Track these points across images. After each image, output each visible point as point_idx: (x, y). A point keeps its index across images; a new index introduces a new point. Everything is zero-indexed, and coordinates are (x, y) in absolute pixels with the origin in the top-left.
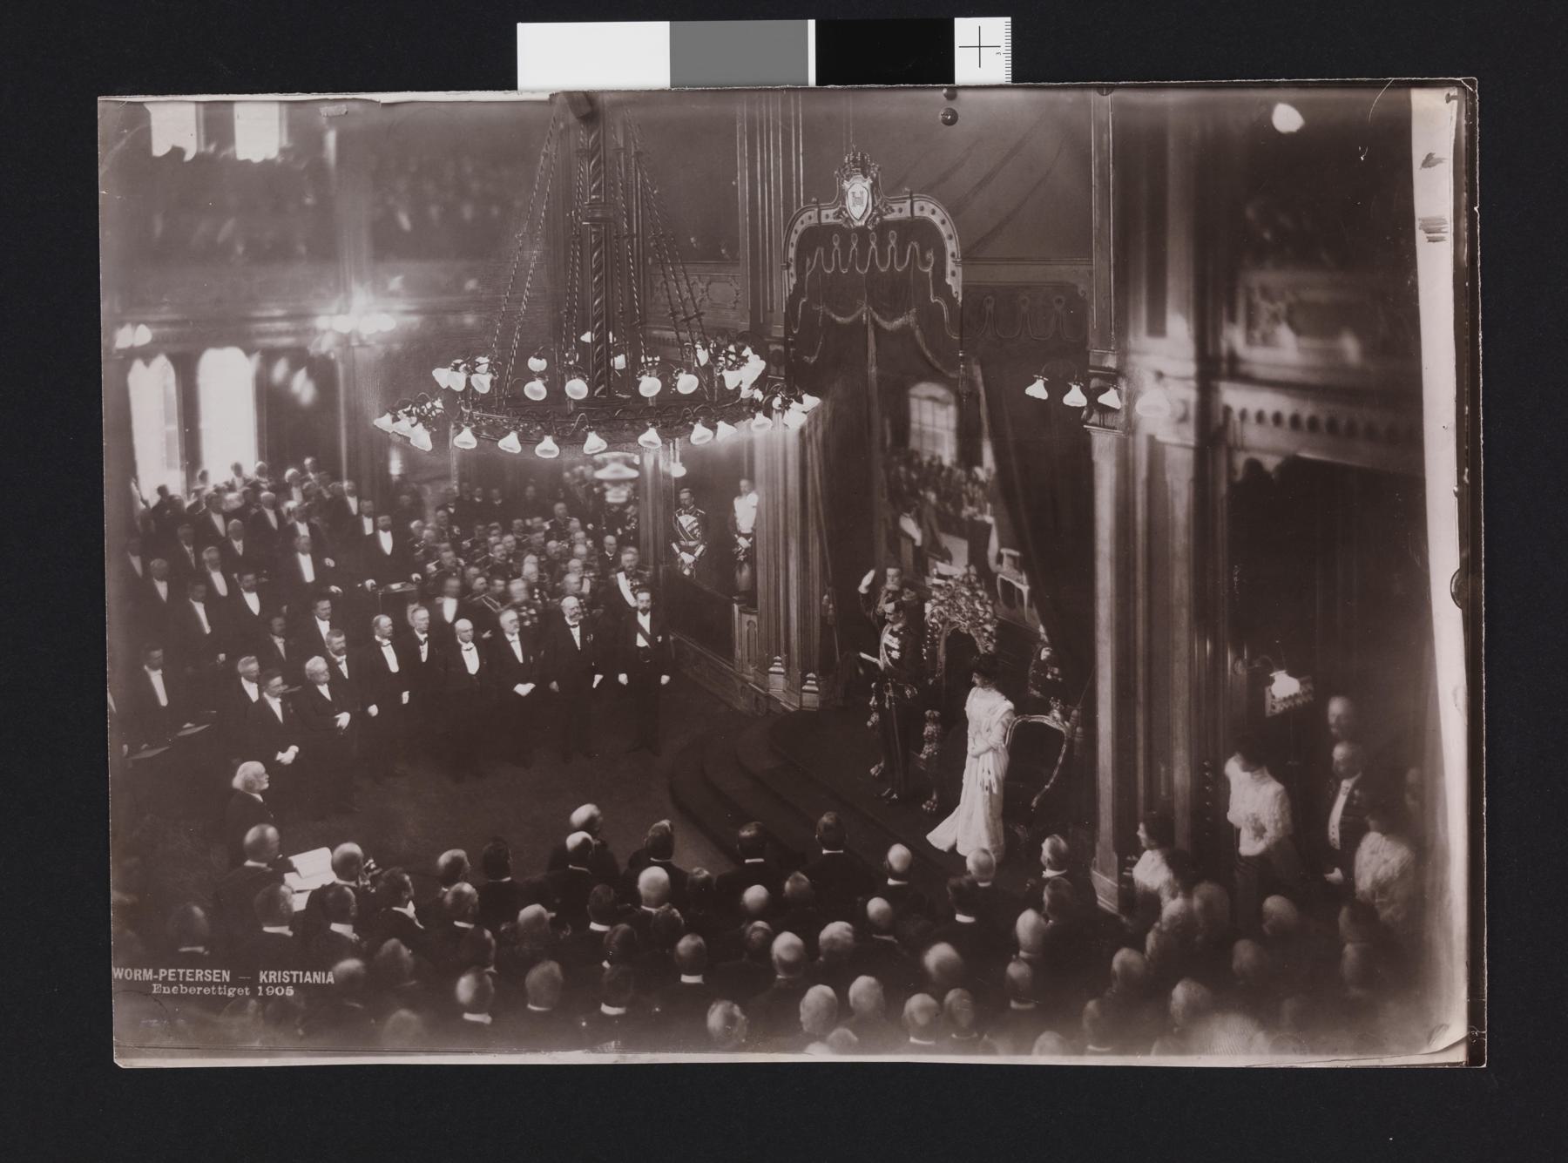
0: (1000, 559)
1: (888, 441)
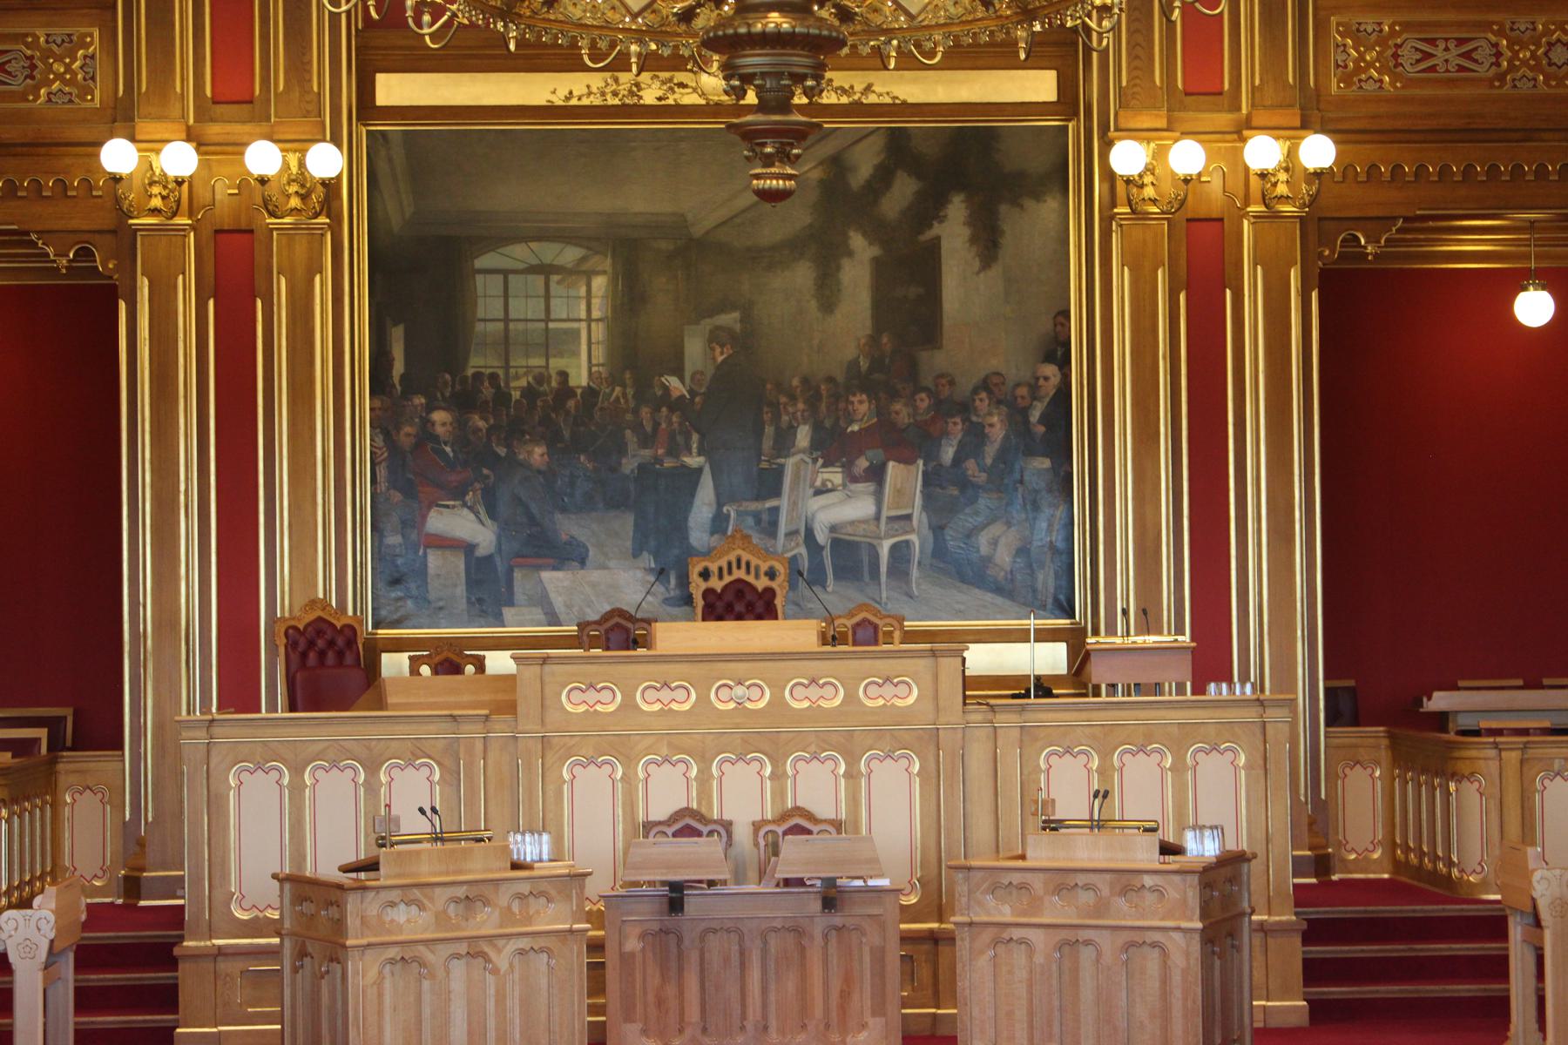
1: (398, 368)
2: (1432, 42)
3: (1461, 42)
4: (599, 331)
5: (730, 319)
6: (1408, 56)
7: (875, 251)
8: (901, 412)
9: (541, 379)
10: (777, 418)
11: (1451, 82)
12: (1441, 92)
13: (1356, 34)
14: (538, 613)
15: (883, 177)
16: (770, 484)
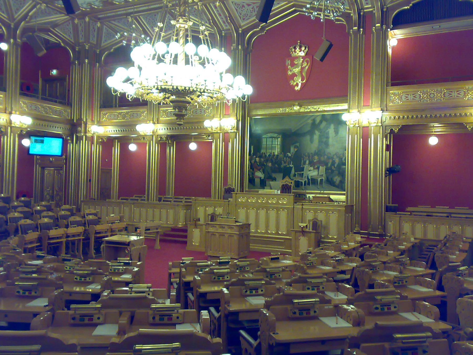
0: (295, 175)
1: (252, 152)
2: (408, 95)
3: (413, 94)
4: (279, 146)
5: (298, 144)
6: (403, 97)
7: (319, 133)
8: (322, 159)
9: (271, 153)
10: (304, 159)
11: (411, 102)
12: (410, 103)
13: (394, 94)
14: (269, 188)
15: (321, 122)
16: (303, 169)
